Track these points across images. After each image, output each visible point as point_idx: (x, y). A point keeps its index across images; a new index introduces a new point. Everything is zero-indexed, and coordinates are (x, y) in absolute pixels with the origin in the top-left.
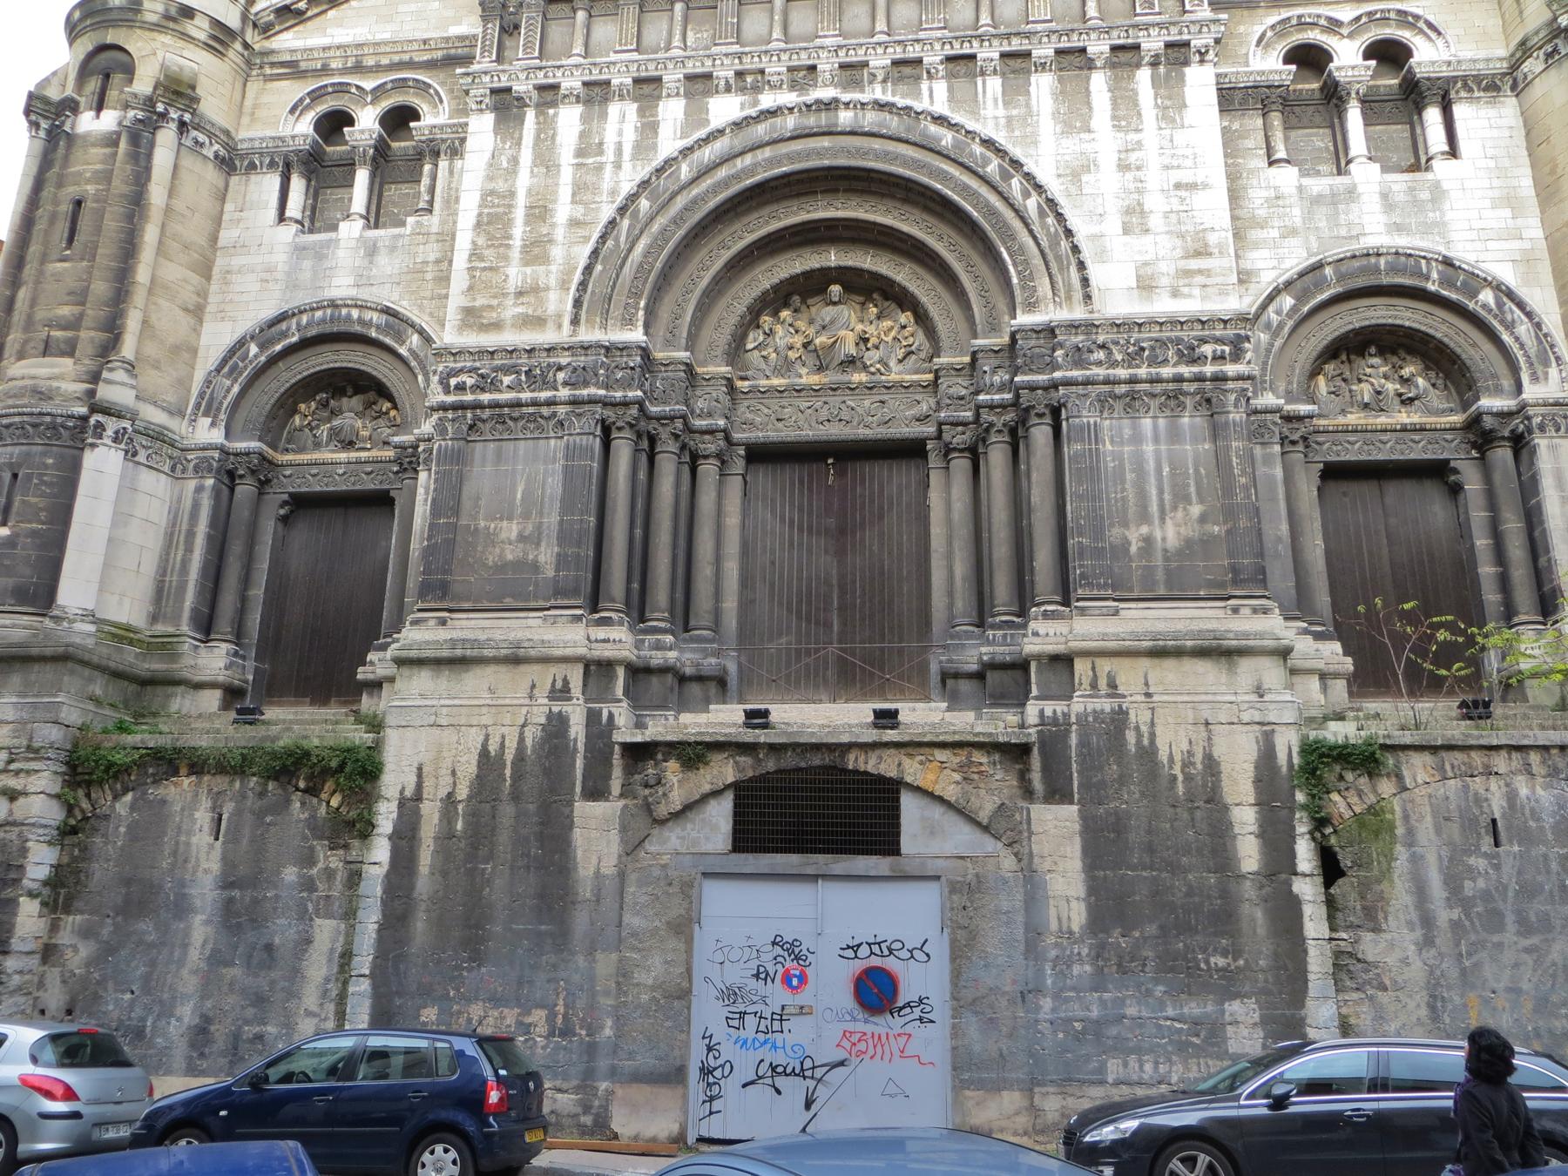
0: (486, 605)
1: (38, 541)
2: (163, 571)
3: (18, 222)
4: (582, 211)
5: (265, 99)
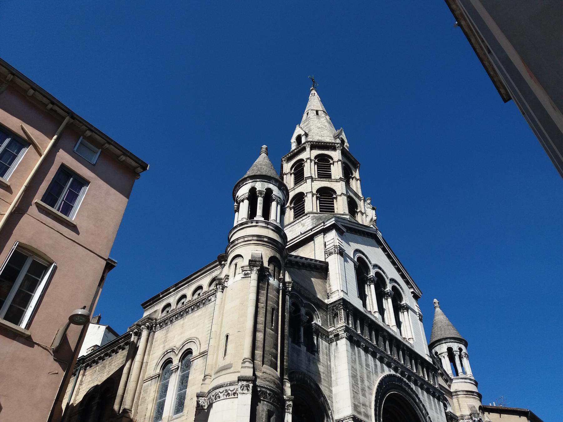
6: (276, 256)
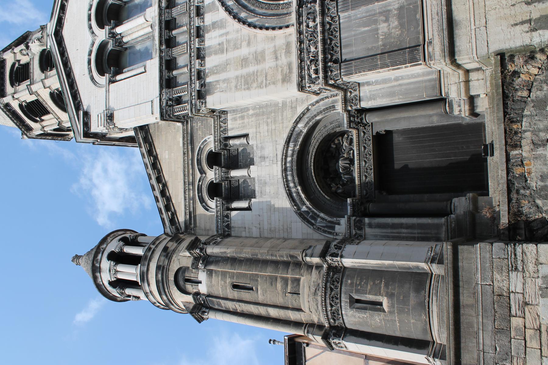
0: (420, 28)
1: (390, 283)
2: (413, 239)
3: (242, 318)
4: (244, 42)
5: (203, 226)
6: (173, 281)
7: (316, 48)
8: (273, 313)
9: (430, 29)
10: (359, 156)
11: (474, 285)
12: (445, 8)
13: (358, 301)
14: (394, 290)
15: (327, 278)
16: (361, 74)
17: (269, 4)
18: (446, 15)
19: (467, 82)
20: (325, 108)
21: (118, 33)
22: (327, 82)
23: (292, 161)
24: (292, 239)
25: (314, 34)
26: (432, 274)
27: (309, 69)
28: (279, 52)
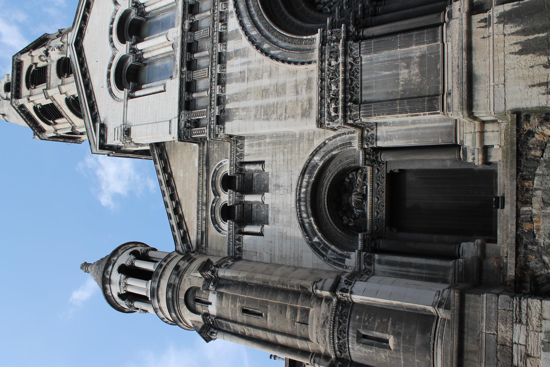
0: (441, 77)
1: (397, 322)
2: (421, 278)
3: (250, 341)
4: (266, 73)
5: (214, 247)
6: (183, 300)
7: (337, 87)
8: (281, 339)
9: (450, 80)
10: (372, 192)
11: (478, 332)
12: (465, 62)
13: (365, 337)
14: (401, 329)
15: (336, 312)
16: (380, 116)
17: (293, 38)
18: (466, 69)
19: (482, 133)
20: (341, 143)
21: (139, 49)
22: (346, 122)
23: (306, 193)
24: (302, 267)
25: (336, 73)
26: (438, 317)
27: (328, 107)
28: (299, 87)
